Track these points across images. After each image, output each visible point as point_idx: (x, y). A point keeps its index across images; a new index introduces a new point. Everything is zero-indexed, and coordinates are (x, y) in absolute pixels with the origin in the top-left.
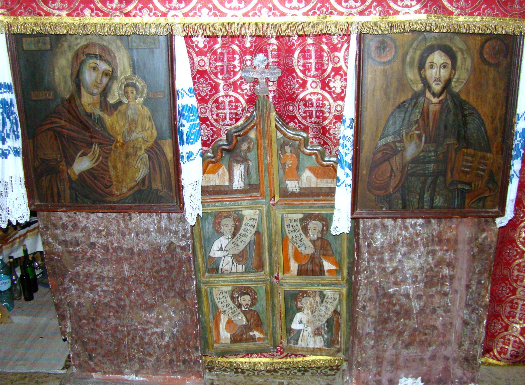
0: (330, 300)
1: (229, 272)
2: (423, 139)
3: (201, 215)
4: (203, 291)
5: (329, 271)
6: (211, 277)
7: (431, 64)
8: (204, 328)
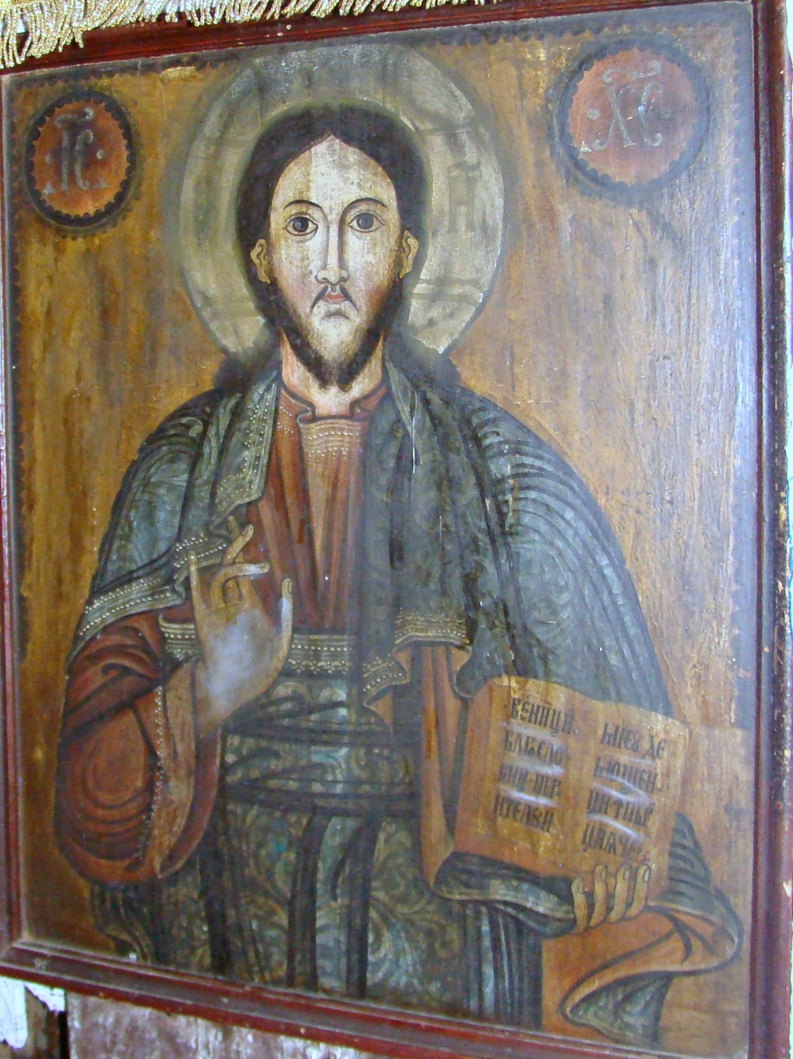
2: (286, 606)
7: (294, 210)
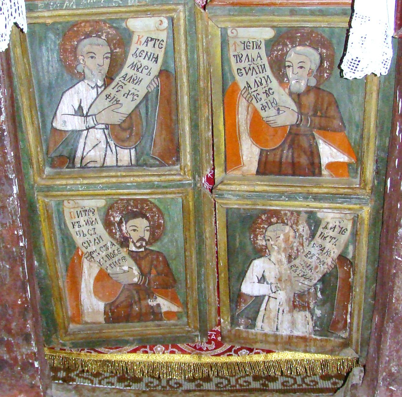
0: (331, 233)
1: (98, 165)
3: (24, 24)
4: (40, 207)
5: (332, 166)
6: (59, 176)
8: (46, 291)
